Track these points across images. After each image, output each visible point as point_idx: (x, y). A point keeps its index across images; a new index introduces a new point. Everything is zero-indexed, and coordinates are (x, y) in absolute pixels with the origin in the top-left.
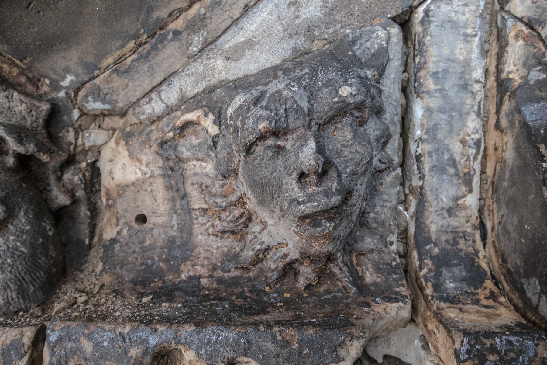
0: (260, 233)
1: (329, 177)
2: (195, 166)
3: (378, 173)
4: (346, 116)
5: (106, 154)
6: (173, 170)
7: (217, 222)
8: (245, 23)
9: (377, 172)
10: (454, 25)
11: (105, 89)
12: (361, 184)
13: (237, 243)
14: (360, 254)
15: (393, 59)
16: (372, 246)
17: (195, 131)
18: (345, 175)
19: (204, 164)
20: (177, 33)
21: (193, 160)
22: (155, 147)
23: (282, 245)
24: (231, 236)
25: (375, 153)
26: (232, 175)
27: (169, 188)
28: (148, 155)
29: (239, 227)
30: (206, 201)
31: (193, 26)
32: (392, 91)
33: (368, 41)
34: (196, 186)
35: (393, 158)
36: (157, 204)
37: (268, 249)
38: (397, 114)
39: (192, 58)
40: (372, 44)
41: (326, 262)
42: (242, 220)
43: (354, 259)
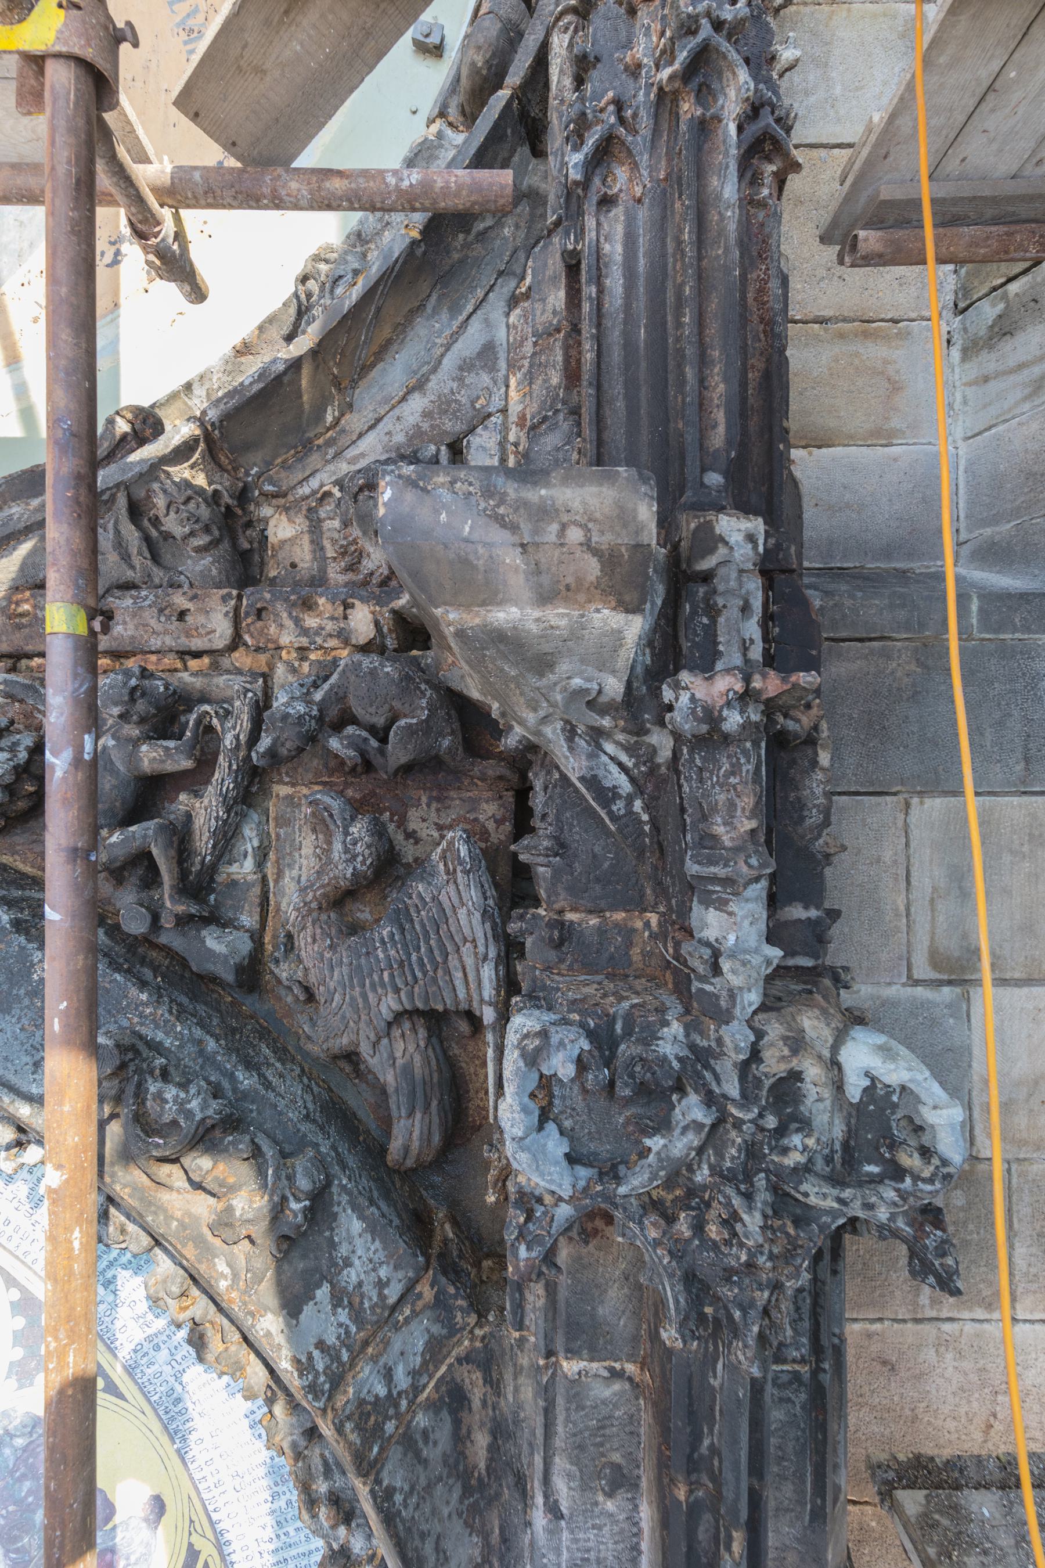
5: (272, 523)
6: (315, 527)
8: (359, 443)
10: (484, 449)
11: (275, 477)
20: (319, 447)
22: (304, 512)
27: (312, 542)
28: (300, 519)
31: (330, 443)
36: (303, 555)
37: (372, 574)
39: (328, 462)
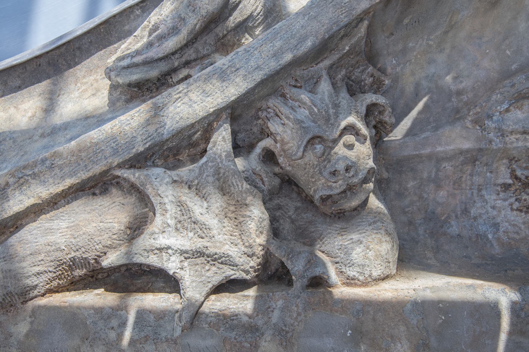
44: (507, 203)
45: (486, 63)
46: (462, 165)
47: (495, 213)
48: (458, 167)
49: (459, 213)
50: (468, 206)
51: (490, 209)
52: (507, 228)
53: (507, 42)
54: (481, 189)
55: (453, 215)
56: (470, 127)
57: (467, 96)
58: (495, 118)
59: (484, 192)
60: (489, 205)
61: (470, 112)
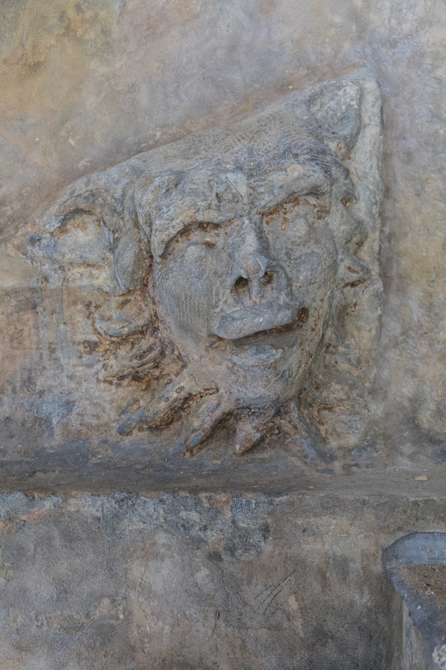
0: (177, 374)
1: (274, 285)
2: (81, 275)
3: (349, 287)
4: (298, 204)
7: (112, 362)
9: (347, 285)
12: (322, 300)
13: (142, 393)
14: (324, 408)
15: (369, 124)
16: (341, 395)
17: (84, 223)
18: (298, 285)
19: (95, 272)
21: (78, 266)
23: (211, 392)
24: (133, 383)
25: (340, 257)
26: (138, 287)
29: (146, 367)
30: (96, 329)
32: (367, 170)
33: (333, 99)
34: (80, 307)
35: (370, 267)
37: (189, 397)
38: (376, 204)
40: (337, 104)
41: (274, 416)
42: (151, 355)
43: (316, 413)
44: (93, 370)
45: (36, 157)
46: (18, 312)
47: (73, 385)
48: (11, 314)
49: (18, 385)
50: (33, 375)
51: (65, 380)
52: (85, 409)
53: (68, 125)
54: (55, 349)
55: (9, 388)
56: (13, 254)
57: (12, 208)
58: (44, 242)
59: (59, 354)
60: (65, 372)
61: (17, 232)
